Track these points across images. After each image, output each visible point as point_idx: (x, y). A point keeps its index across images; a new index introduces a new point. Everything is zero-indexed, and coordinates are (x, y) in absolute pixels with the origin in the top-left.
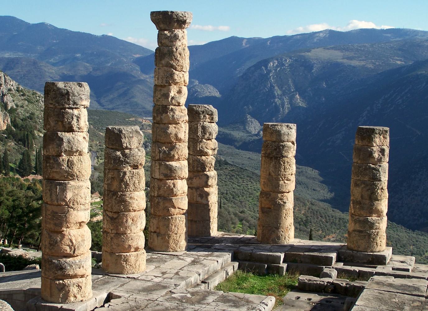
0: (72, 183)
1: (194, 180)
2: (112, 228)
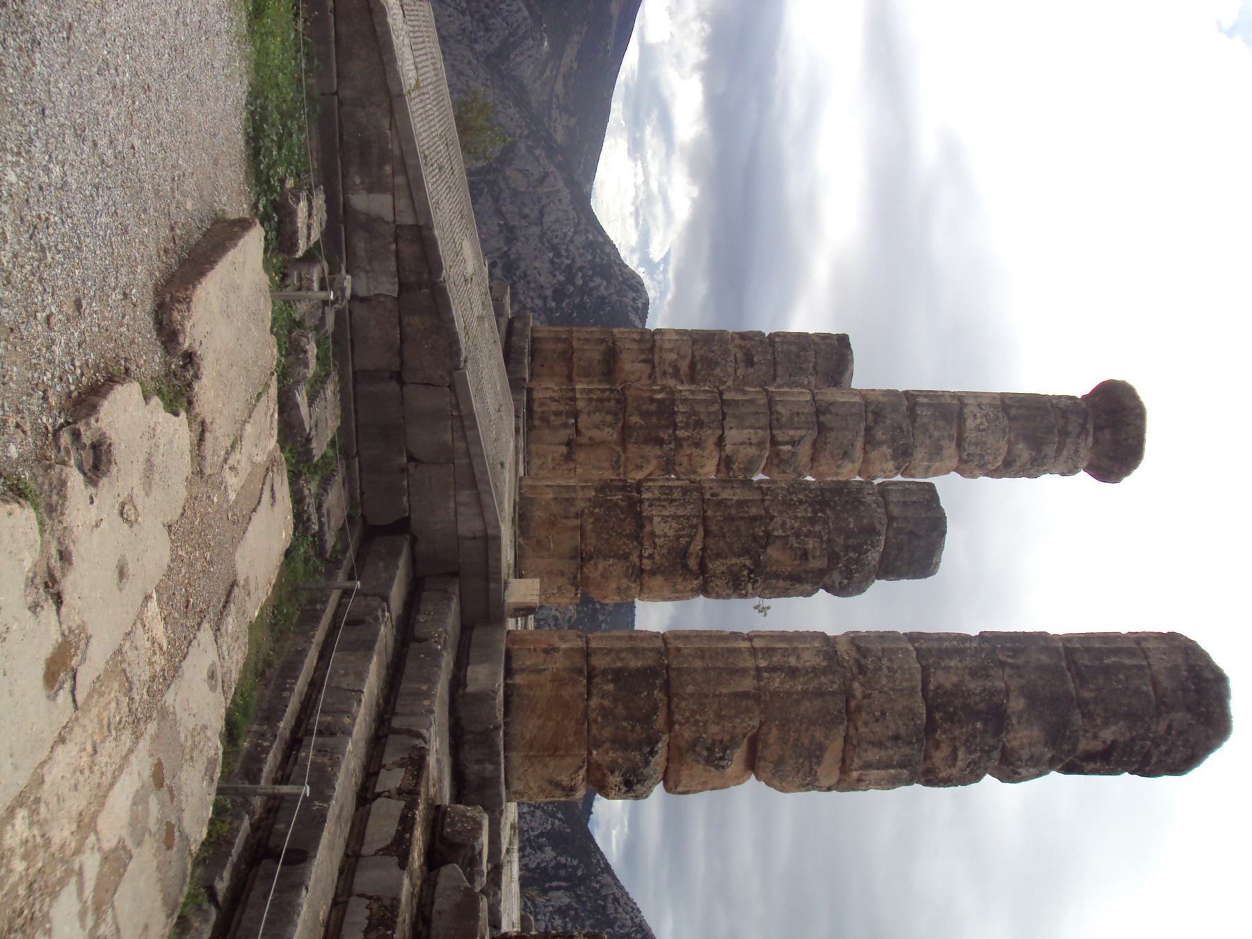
2: (657, 557)
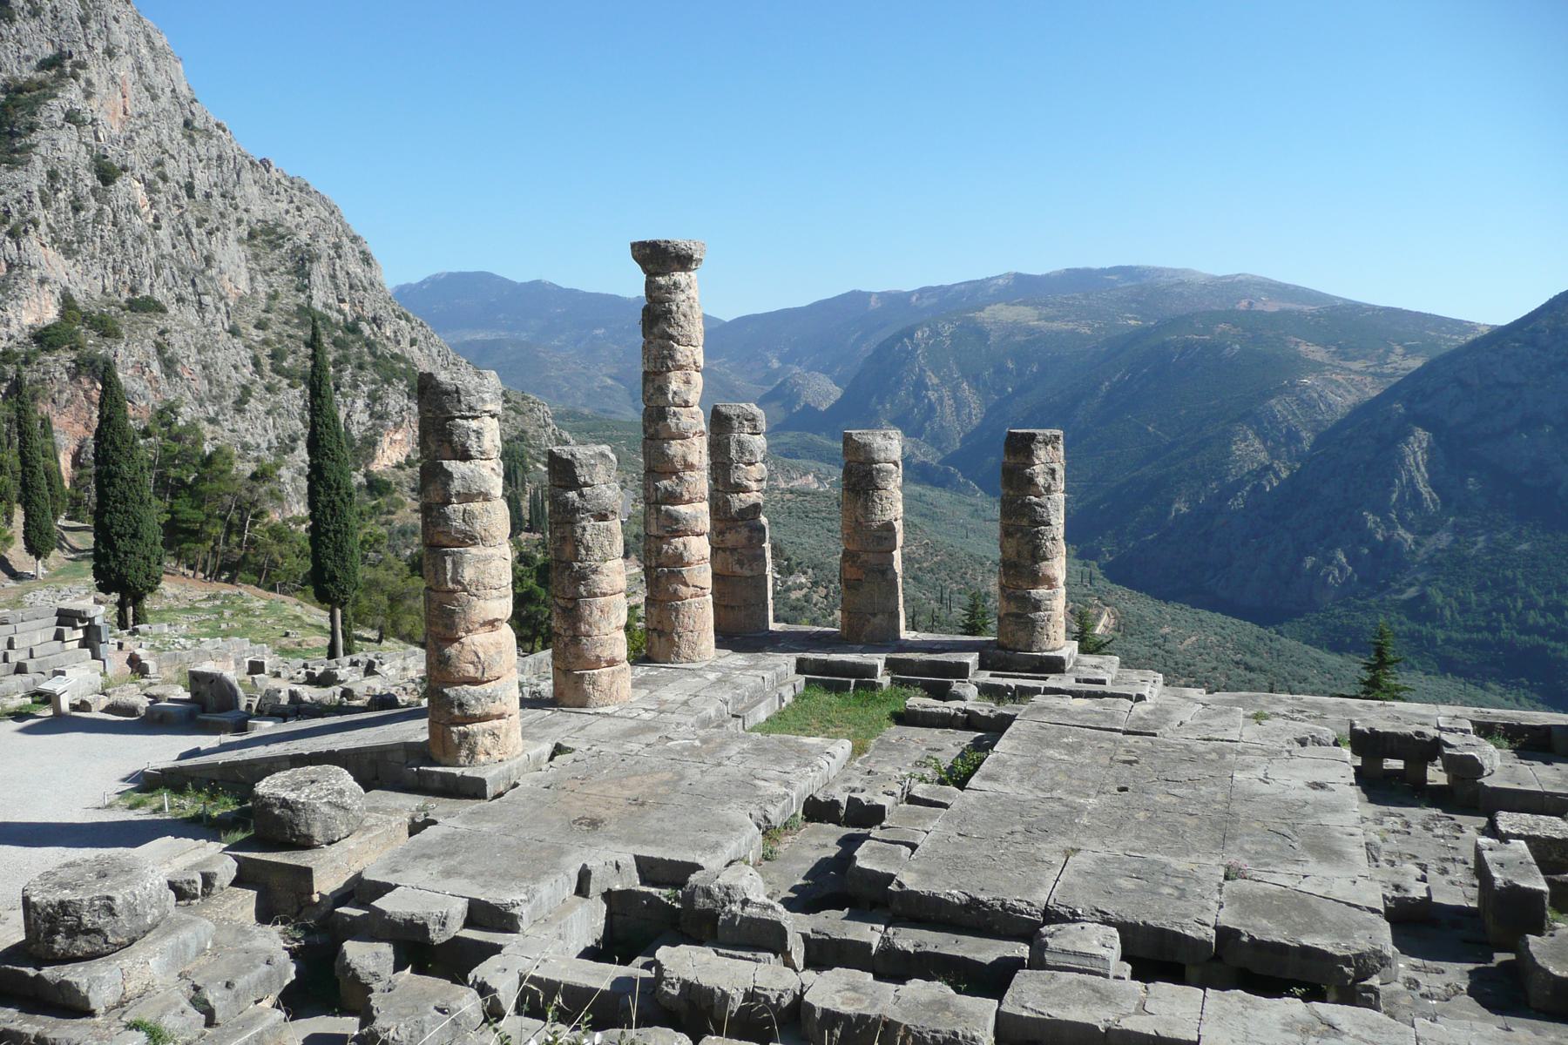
0: (473, 550)
1: (728, 536)
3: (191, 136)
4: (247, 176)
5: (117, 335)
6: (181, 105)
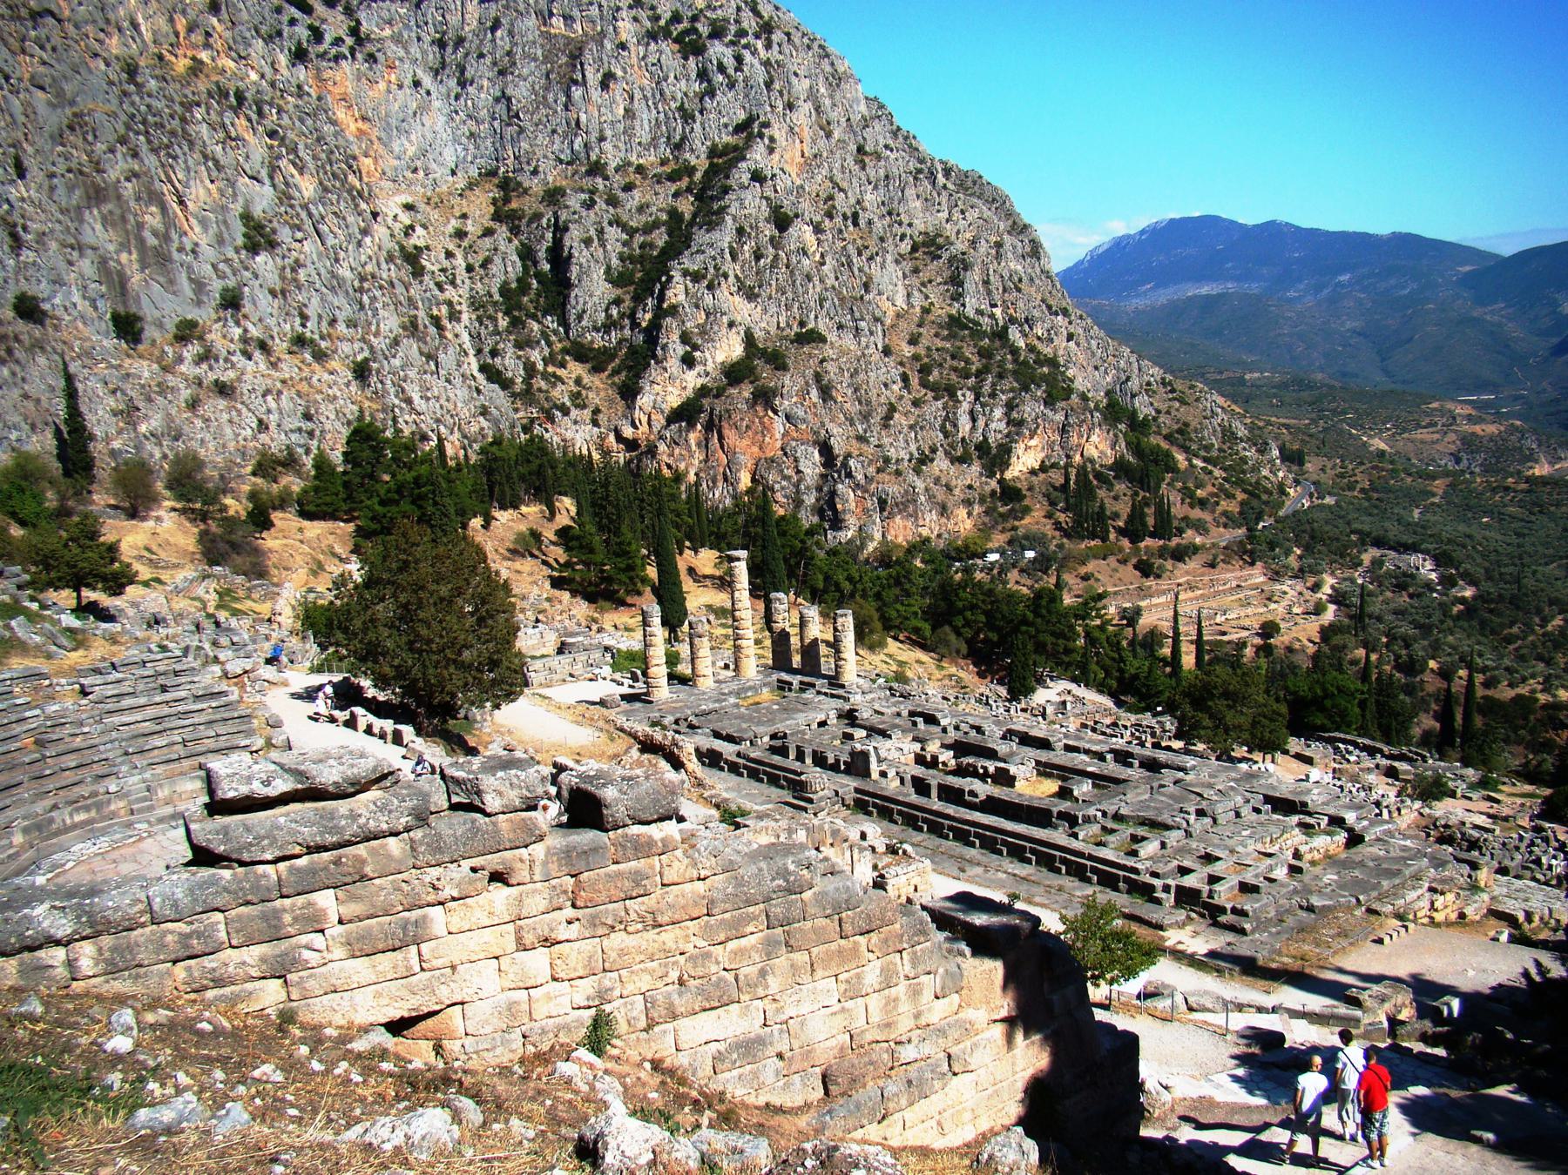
3: (862, 161)
4: (910, 192)
5: (782, 367)
6: (855, 133)
